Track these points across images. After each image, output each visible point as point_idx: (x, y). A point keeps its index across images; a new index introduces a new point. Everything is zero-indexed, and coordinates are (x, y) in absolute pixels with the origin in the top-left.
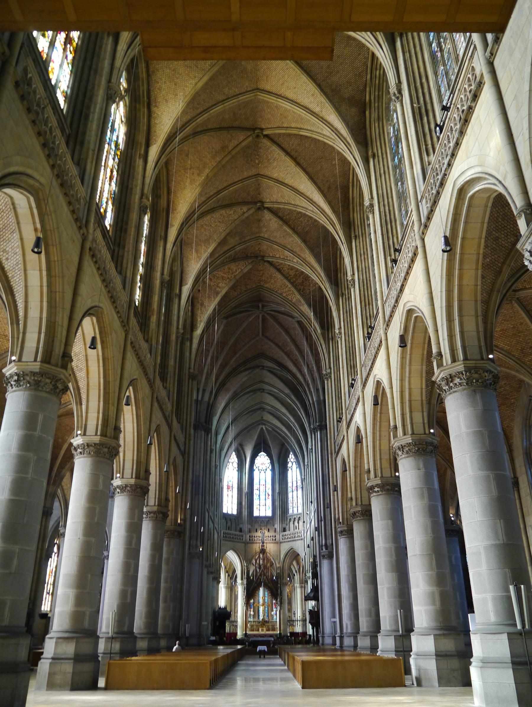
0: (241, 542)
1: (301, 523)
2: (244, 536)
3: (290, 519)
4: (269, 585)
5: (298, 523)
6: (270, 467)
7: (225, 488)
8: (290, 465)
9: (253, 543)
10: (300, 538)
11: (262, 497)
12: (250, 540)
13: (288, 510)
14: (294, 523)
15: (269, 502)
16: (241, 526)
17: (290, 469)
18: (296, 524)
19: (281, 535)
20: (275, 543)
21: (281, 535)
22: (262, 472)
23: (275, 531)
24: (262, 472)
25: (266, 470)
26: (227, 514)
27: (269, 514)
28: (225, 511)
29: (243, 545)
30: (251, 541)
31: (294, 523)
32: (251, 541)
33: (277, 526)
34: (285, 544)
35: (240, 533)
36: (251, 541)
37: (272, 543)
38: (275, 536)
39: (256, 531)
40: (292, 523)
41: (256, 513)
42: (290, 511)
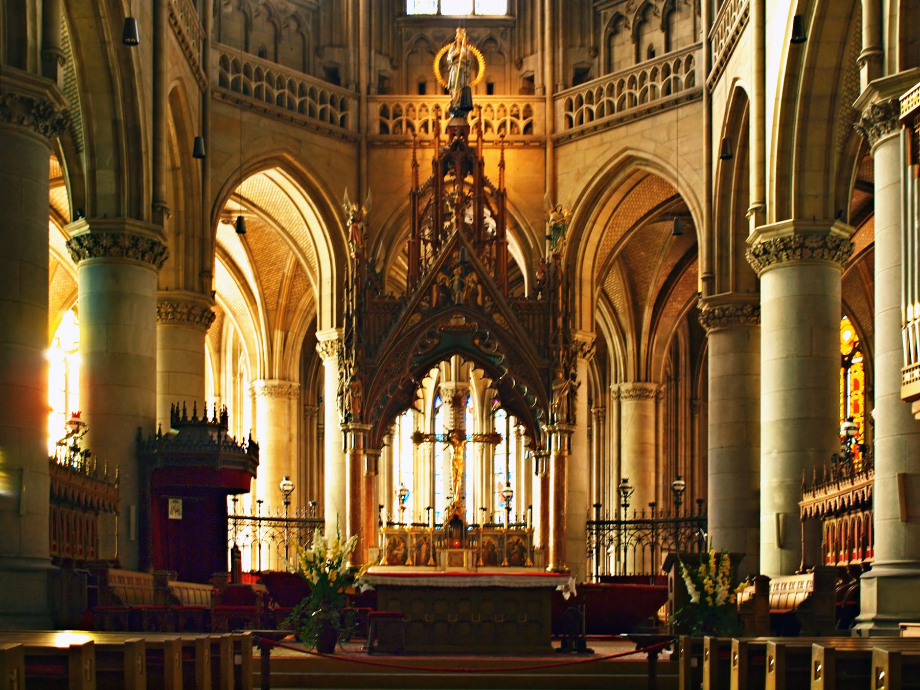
0: (331, 134)
1: (682, 28)
2: (352, 104)
3: (618, 17)
5: (667, 28)
9: (403, 144)
10: (684, 92)
12: (384, 128)
14: (637, 38)
16: (336, 56)
18: (654, 36)
19: (561, 103)
20: (526, 145)
21: (561, 103)
23: (528, 85)
29: (346, 149)
30: (393, 136)
31: (637, 38)
32: (391, 136)
33: (540, 64)
34: (583, 144)
35: (330, 89)
36: (391, 136)
37: (511, 144)
38: (528, 111)
39: (422, 90)
40: (627, 34)
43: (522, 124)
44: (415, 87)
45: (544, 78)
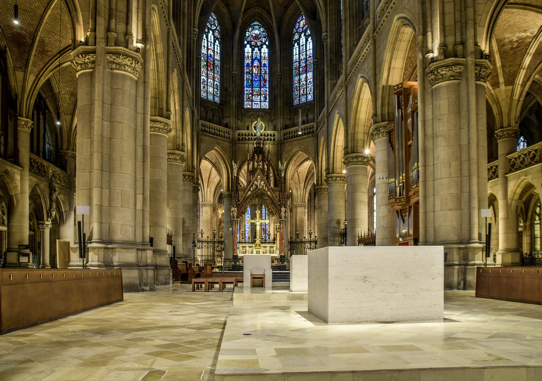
4: (269, 193)
6: (267, 43)
7: (203, 63)
8: (296, 37)
11: (256, 84)
13: (292, 100)
15: (266, 90)
17: (296, 44)
22: (256, 49)
24: (256, 49)
25: (262, 46)
26: (207, 101)
27: (266, 105)
28: (203, 95)
41: (247, 105)
42: (296, 102)
43: (272, 138)
44: (246, 129)
45: (279, 126)
